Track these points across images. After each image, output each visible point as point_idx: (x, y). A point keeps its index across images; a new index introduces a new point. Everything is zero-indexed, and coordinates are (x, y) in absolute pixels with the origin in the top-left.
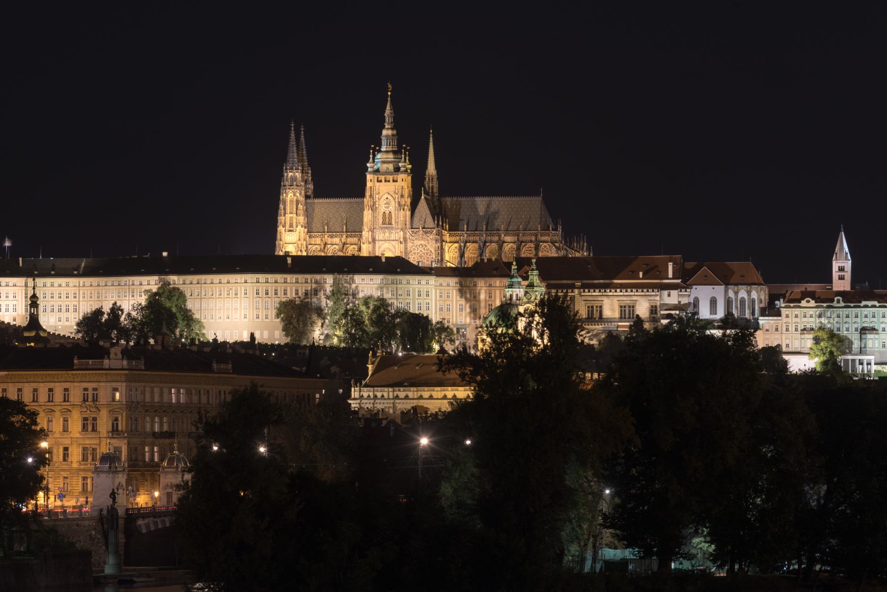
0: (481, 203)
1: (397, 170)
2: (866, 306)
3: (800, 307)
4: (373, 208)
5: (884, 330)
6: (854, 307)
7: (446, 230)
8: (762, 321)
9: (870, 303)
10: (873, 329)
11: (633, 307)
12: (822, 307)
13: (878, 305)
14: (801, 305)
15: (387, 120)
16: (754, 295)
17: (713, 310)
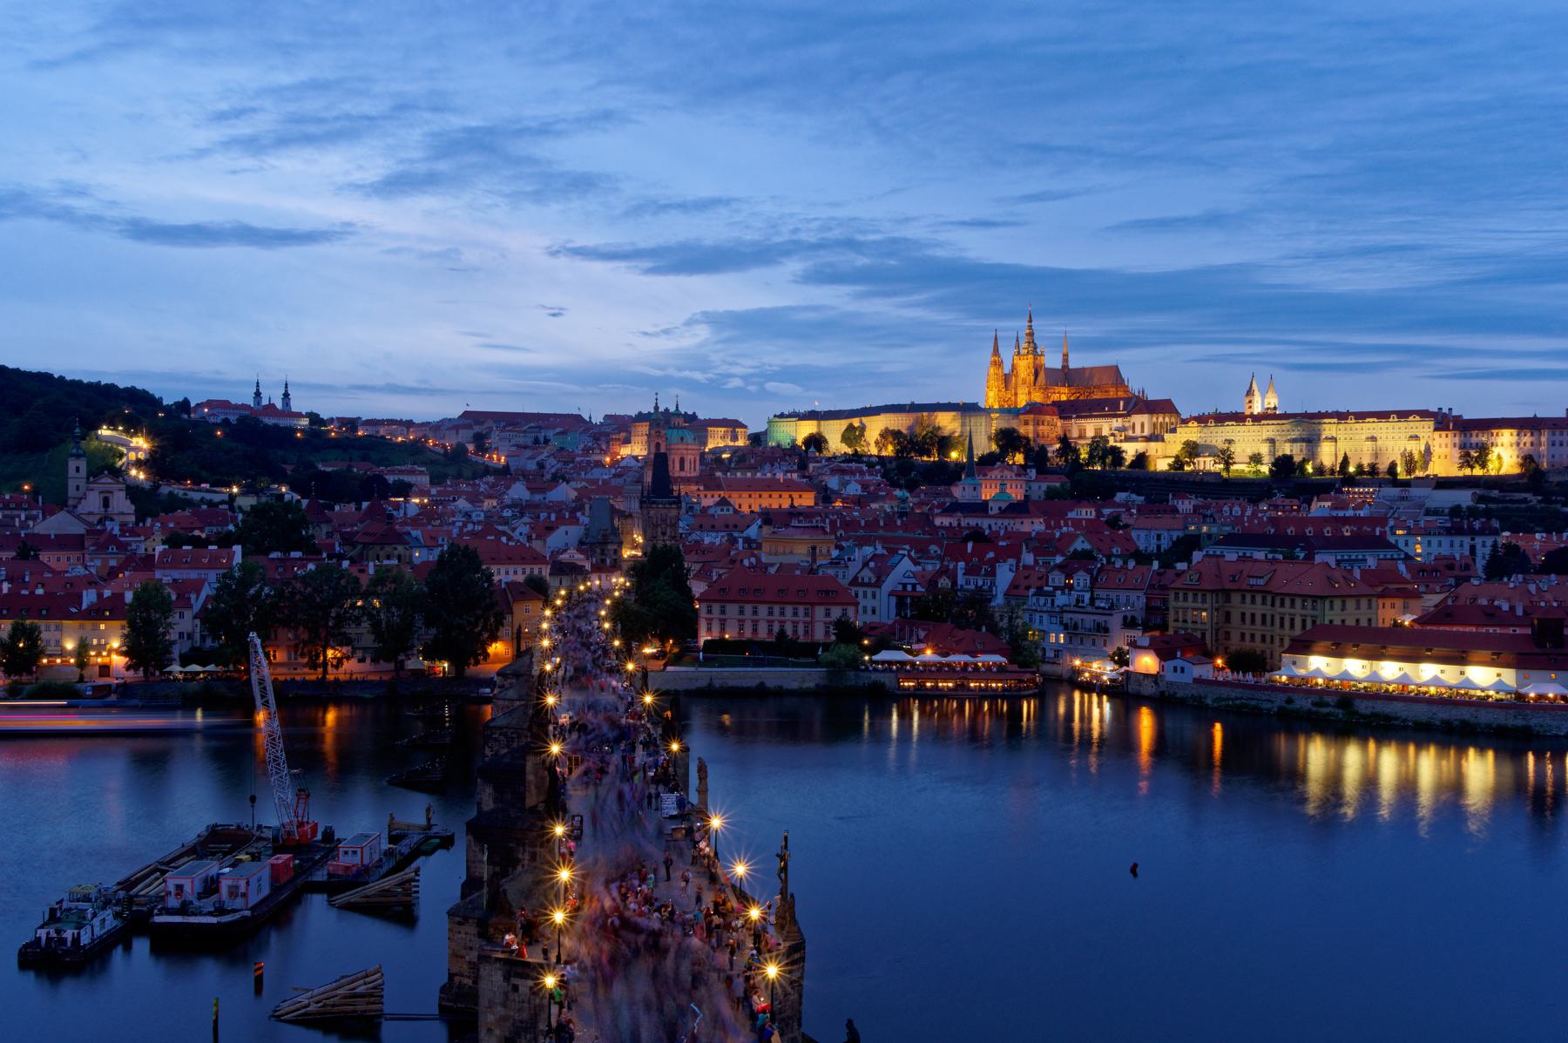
8: (1167, 436)
9: (1230, 423)
16: (1167, 420)
17: (1143, 431)
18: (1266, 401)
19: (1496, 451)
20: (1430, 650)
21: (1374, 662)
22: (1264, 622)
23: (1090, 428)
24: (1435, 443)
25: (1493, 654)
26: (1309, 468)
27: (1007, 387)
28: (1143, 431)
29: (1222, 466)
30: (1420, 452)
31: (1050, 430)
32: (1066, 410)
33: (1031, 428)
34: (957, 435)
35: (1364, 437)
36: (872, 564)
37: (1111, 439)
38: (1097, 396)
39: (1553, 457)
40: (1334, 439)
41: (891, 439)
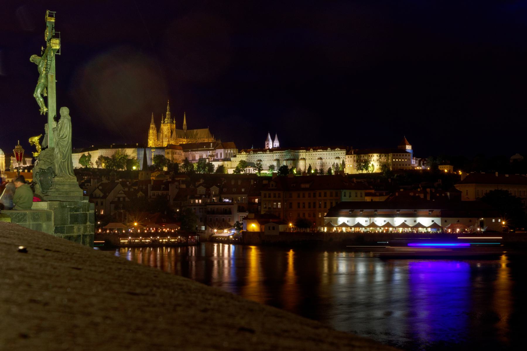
0: (195, 131)
1: (168, 123)
2: (259, 153)
3: (241, 154)
4: (163, 134)
5: (264, 160)
6: (256, 154)
7: (185, 138)
8: (232, 159)
9: (260, 153)
10: (261, 161)
11: (202, 156)
12: (247, 154)
13: (262, 153)
14: (242, 154)
15: (168, 110)
16: (232, 151)
17: (221, 157)
18: (274, 144)
19: (372, 163)
20: (399, 211)
21: (372, 218)
22: (310, 207)
23: (197, 155)
24: (347, 160)
25: (430, 211)
26: (295, 171)
27: (158, 139)
28: (221, 157)
29: (257, 171)
30: (341, 164)
31: (180, 156)
32: (185, 148)
33: (170, 155)
34: (135, 159)
35: (317, 158)
36: (100, 187)
37: (207, 161)
38: (200, 141)
39: (394, 165)
40: (304, 159)
41: (103, 161)
